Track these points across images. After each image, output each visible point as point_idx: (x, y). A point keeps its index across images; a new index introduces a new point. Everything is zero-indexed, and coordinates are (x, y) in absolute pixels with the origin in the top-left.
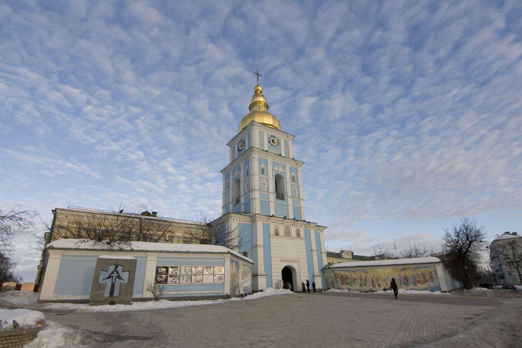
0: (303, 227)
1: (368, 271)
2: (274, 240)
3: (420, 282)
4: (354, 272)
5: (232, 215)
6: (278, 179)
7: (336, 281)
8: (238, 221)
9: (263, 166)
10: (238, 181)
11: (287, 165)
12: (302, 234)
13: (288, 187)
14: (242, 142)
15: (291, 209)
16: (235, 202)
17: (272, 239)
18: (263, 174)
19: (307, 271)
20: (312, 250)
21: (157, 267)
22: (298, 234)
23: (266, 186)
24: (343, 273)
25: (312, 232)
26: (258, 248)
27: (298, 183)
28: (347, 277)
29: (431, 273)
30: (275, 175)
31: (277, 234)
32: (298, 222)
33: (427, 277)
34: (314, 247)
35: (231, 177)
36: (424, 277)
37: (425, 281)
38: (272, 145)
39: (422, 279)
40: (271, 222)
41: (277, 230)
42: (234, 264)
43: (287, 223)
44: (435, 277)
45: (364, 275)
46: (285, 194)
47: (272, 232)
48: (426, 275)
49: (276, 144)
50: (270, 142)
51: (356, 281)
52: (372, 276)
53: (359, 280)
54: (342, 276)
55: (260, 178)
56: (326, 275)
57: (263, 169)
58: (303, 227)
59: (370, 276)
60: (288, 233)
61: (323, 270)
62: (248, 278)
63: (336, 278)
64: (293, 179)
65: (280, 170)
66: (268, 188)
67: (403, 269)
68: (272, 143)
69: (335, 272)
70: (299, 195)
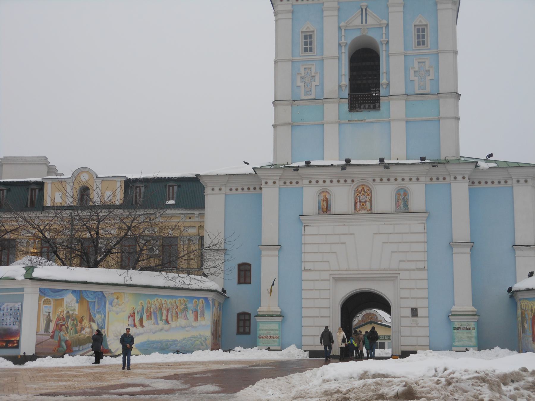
7: (523, 327)
18: (308, 47)
20: (472, 244)
23: (317, 83)
25: (460, 190)
30: (349, 38)
31: (325, 208)
32: (392, 169)
40: (306, 182)
41: (327, 200)
46: (382, 92)
58: (422, 179)
63: (524, 319)
69: (524, 303)
70: (436, 81)
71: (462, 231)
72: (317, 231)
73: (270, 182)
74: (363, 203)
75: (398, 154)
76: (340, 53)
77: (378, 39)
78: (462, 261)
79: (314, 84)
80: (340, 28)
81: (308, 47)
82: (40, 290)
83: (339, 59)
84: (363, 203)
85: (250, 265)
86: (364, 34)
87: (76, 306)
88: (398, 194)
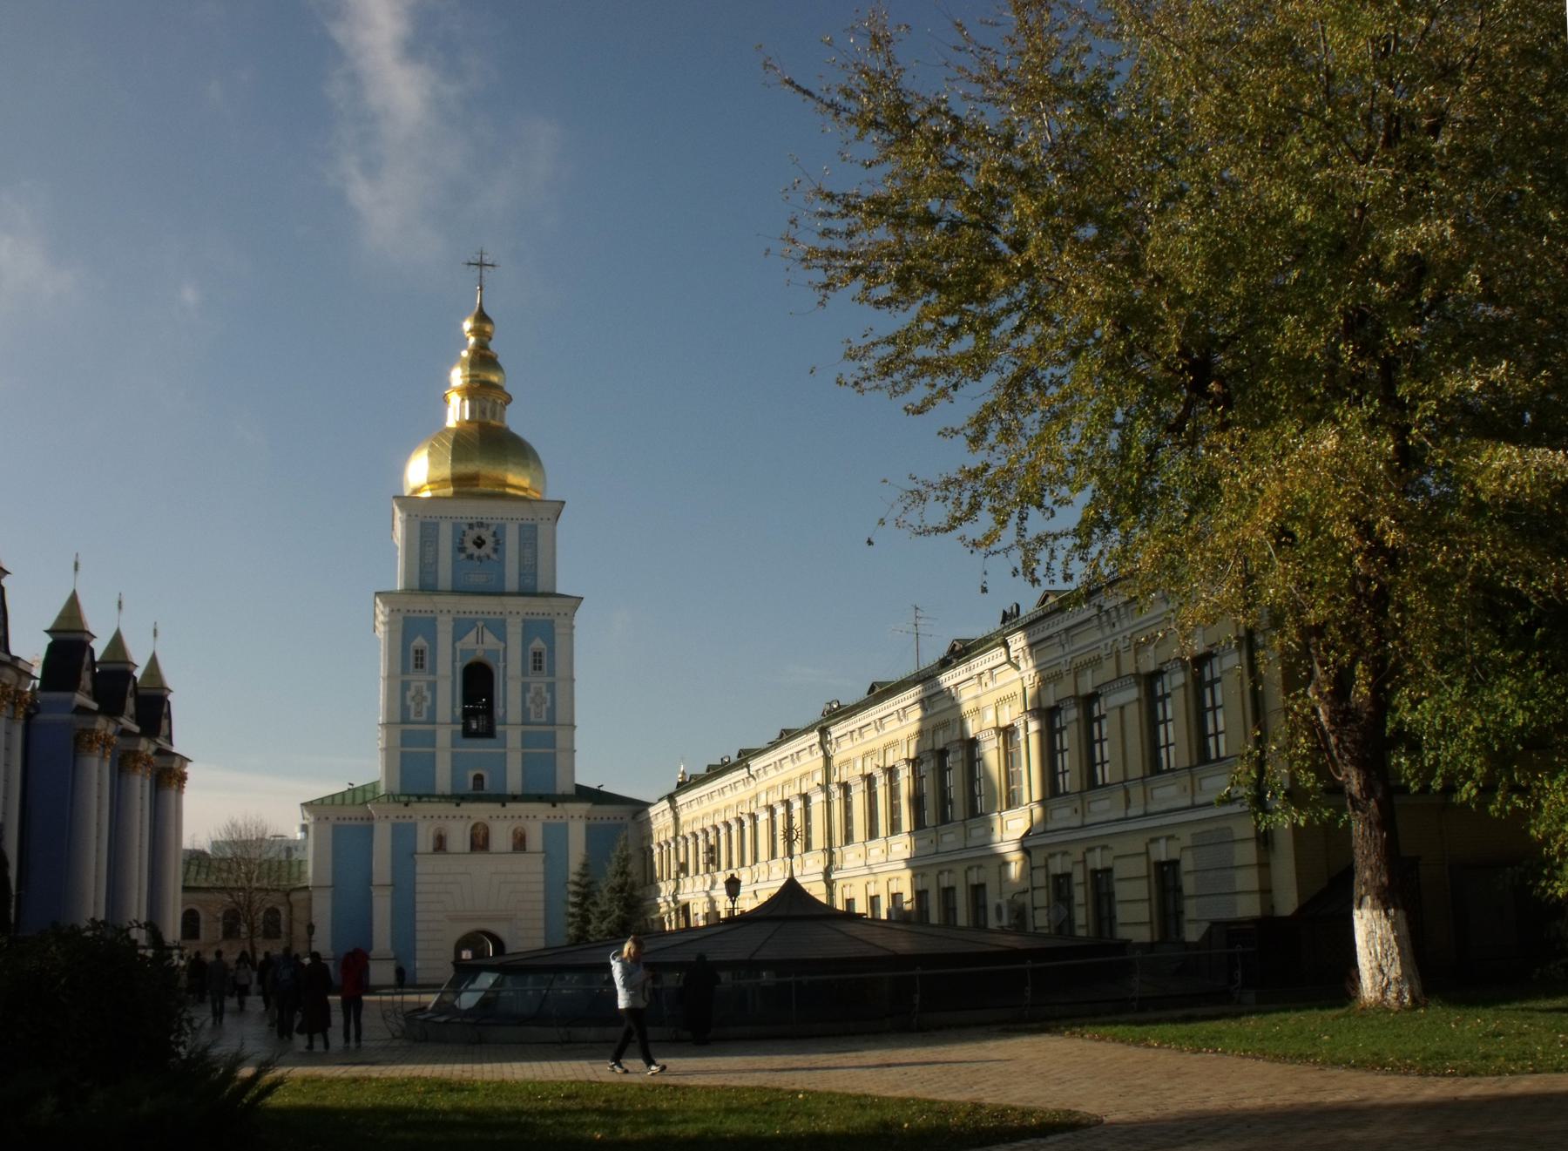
2: (428, 868)
12: (535, 840)
13: (510, 698)
18: (419, 664)
22: (520, 843)
27: (552, 673)
31: (440, 844)
38: (471, 557)
43: (480, 812)
47: (425, 842)
49: (487, 549)
50: (462, 549)
57: (419, 654)
60: (480, 842)
64: (537, 662)
65: (490, 640)
66: (433, 710)
68: (471, 548)
70: (552, 710)
75: (514, 784)
76: (454, 673)
79: (425, 705)
80: (454, 648)
81: (419, 664)
83: (454, 683)
88: (515, 833)
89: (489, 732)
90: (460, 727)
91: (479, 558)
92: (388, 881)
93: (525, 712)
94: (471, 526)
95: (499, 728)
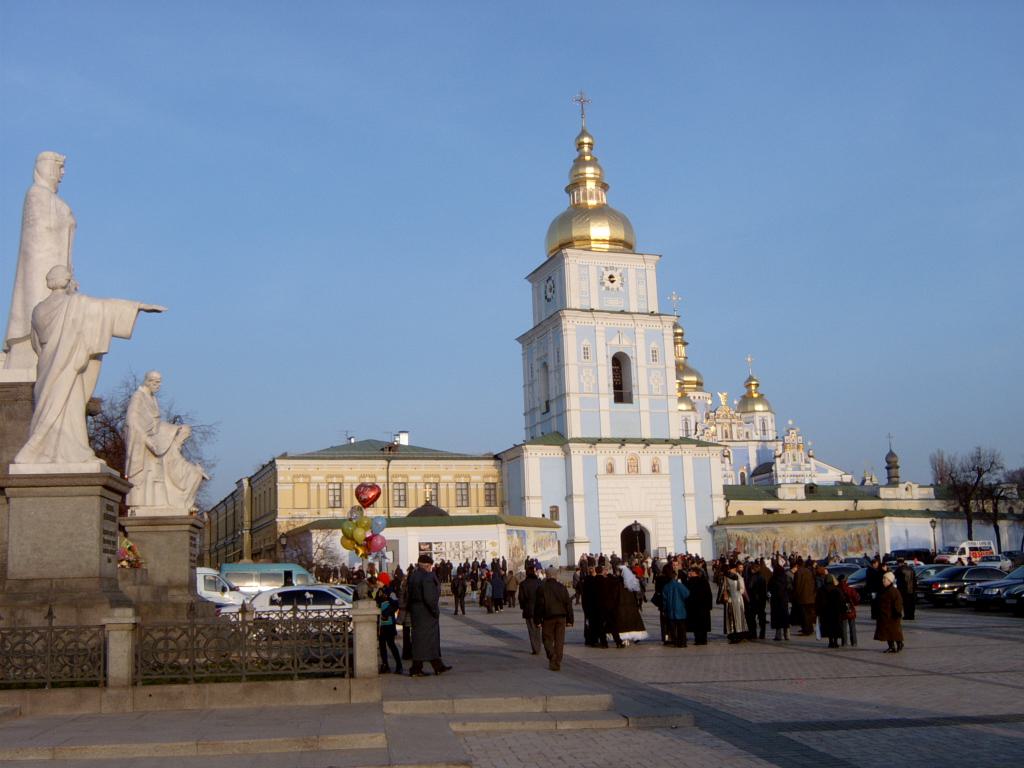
0: (668, 453)
1: (779, 530)
3: (852, 550)
4: (757, 532)
5: (527, 446)
6: (619, 363)
8: (539, 454)
9: (586, 342)
10: (545, 365)
11: (639, 330)
12: (665, 467)
14: (550, 282)
15: (645, 418)
16: (544, 409)
17: (602, 483)
19: (671, 532)
21: (420, 544)
24: (741, 533)
25: (688, 461)
26: (575, 500)
28: (746, 541)
29: (870, 534)
31: (611, 470)
32: (652, 446)
33: (864, 542)
34: (690, 487)
35: (535, 356)
36: (859, 542)
37: (861, 548)
38: (608, 288)
39: (855, 544)
40: (599, 452)
41: (611, 464)
42: (515, 535)
44: (875, 540)
45: (772, 537)
47: (602, 469)
48: (862, 538)
50: (602, 284)
51: (759, 548)
52: (784, 538)
53: (764, 546)
54: (738, 539)
55: (580, 369)
56: (717, 536)
59: (781, 540)
61: (711, 527)
62: (548, 549)
67: (831, 528)
68: (608, 283)
71: (690, 487)
72: (605, 483)
73: (577, 452)
74: (633, 468)
75: (647, 435)
77: (630, 355)
78: (691, 505)
82: (508, 531)
84: (633, 468)
85: (556, 507)
86: (621, 350)
87: (517, 540)
89: (630, 401)
90: (613, 396)
91: (613, 289)
92: (582, 493)
93: (650, 386)
94: (606, 268)
95: (635, 397)
